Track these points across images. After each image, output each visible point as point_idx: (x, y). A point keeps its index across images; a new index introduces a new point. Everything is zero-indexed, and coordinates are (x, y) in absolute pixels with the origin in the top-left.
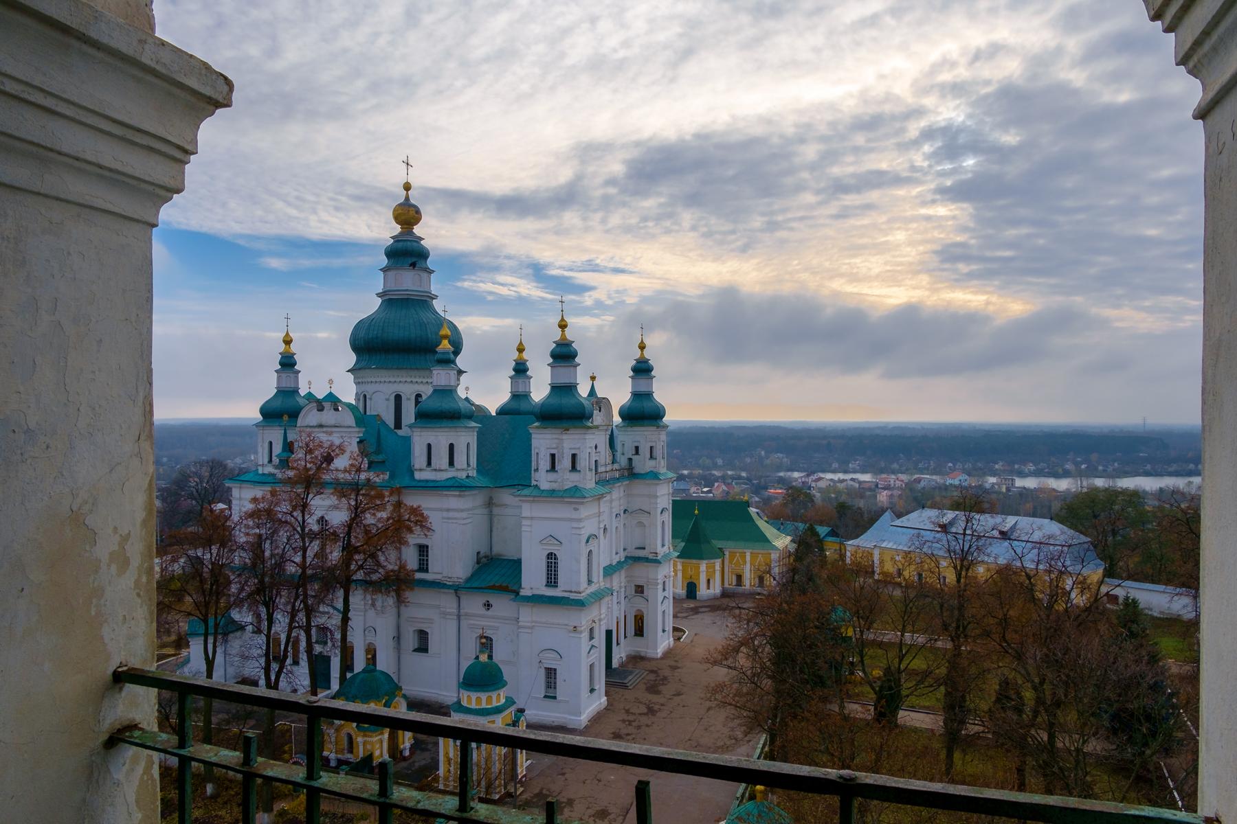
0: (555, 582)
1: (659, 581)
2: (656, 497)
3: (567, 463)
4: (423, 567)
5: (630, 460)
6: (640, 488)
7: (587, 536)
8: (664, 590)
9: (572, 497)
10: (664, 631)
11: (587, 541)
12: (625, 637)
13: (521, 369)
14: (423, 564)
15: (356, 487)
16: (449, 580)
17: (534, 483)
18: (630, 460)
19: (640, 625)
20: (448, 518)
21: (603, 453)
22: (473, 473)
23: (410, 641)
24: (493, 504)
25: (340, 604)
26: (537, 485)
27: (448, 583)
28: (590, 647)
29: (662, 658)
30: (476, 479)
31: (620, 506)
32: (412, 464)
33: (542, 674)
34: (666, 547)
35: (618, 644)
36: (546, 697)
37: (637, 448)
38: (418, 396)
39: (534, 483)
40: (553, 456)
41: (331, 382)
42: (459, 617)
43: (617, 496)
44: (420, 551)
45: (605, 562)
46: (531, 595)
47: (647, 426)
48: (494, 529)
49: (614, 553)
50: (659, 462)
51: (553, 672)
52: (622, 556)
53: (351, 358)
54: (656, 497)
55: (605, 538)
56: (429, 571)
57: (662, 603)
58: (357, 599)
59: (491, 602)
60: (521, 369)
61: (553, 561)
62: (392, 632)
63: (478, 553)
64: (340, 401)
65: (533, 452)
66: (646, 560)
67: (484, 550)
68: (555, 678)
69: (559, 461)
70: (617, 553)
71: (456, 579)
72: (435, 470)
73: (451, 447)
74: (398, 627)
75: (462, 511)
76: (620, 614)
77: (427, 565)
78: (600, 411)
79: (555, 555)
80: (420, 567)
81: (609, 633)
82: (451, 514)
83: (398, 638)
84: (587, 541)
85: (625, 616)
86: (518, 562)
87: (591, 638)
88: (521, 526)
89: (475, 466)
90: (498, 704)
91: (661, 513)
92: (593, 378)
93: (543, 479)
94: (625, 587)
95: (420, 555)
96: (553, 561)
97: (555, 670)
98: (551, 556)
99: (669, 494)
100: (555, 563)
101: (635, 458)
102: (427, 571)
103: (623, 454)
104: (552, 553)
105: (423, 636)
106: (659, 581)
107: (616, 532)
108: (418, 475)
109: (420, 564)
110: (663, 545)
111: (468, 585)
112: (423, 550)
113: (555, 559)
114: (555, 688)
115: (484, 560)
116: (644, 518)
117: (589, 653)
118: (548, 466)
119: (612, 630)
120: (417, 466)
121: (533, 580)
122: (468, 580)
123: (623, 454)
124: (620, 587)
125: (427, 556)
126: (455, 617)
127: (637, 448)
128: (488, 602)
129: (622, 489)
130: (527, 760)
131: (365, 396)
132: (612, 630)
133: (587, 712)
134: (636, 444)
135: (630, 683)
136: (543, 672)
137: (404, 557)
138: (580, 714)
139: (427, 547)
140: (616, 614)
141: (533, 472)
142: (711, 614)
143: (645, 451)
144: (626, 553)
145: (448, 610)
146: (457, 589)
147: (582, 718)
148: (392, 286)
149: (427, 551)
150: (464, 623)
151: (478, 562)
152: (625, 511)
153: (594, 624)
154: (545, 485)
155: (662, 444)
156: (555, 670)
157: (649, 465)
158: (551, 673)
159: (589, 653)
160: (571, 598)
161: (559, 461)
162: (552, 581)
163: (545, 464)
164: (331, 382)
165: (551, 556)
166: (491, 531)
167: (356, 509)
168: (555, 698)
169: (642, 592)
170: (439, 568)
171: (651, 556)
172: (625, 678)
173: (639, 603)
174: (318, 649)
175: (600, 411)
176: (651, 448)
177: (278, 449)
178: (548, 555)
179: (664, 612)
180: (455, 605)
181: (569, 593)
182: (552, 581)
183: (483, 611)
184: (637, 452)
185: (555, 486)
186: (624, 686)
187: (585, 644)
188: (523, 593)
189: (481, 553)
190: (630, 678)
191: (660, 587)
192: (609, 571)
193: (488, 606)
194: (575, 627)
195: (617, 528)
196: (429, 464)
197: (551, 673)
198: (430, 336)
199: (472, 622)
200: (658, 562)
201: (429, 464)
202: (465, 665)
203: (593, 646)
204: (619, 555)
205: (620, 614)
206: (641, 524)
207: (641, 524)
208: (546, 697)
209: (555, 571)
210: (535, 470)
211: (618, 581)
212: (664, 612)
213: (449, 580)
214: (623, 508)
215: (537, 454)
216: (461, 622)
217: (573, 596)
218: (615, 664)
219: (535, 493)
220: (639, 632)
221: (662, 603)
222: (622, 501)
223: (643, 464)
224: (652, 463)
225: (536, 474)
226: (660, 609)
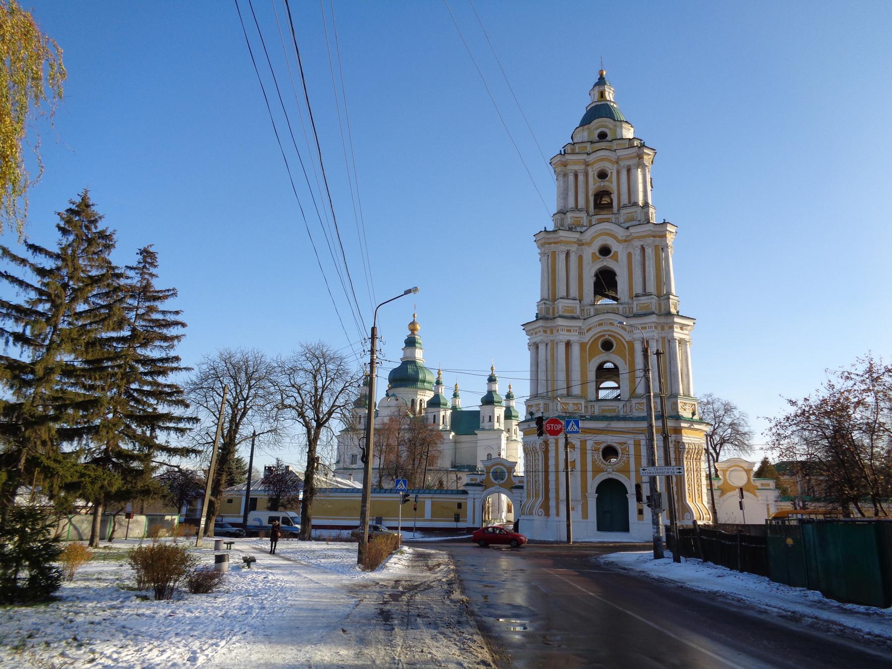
38: (421, 400)
40: (490, 417)
148: (408, 354)
163: (487, 419)
185: (491, 428)
196: (434, 422)
201: (434, 422)
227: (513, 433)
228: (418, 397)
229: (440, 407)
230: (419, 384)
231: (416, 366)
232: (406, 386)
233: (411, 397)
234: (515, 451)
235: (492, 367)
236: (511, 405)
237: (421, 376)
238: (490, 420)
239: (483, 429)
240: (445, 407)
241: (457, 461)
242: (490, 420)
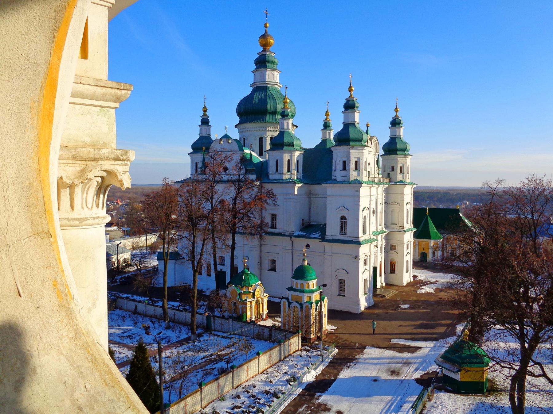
0: (345, 233)
3: (353, 166)
4: (274, 226)
8: (408, 248)
10: (407, 272)
11: (363, 210)
12: (385, 274)
13: (326, 126)
14: (274, 225)
15: (239, 181)
16: (287, 232)
17: (333, 178)
18: (389, 174)
19: (393, 267)
20: (287, 199)
23: (267, 265)
24: (311, 194)
25: (230, 243)
26: (335, 179)
27: (286, 234)
28: (364, 269)
29: (405, 286)
32: (268, 172)
35: (380, 275)
39: (333, 178)
40: (344, 162)
41: (226, 128)
42: (292, 253)
44: (272, 218)
45: (373, 229)
46: (331, 239)
48: (312, 208)
49: (379, 224)
50: (406, 176)
53: (237, 120)
55: (374, 216)
56: (277, 227)
57: (406, 255)
58: (238, 238)
60: (326, 126)
61: (344, 220)
62: (257, 260)
63: (303, 220)
64: (230, 138)
65: (333, 161)
67: (306, 218)
68: (344, 285)
69: (348, 164)
71: (291, 232)
72: (280, 174)
73: (289, 162)
74: (261, 258)
76: (381, 259)
77: (276, 225)
78: (372, 144)
79: (345, 217)
80: (272, 227)
81: (375, 269)
83: (260, 264)
84: (363, 210)
85: (385, 262)
89: (302, 173)
90: (313, 288)
91: (407, 204)
92: (367, 125)
93: (338, 174)
95: (272, 220)
96: (344, 220)
98: (343, 218)
100: (345, 221)
101: (392, 173)
102: (276, 228)
104: (343, 216)
105: (273, 262)
108: (271, 177)
109: (272, 225)
112: (274, 217)
113: (345, 220)
114: (344, 291)
115: (306, 224)
117: (364, 272)
118: (341, 167)
120: (270, 172)
121: (333, 230)
123: (385, 171)
125: (276, 220)
128: (308, 244)
131: (244, 139)
137: (263, 216)
139: (276, 215)
140: (379, 260)
141: (333, 172)
149: (276, 218)
151: (303, 224)
153: (366, 257)
154: (339, 179)
157: (400, 177)
158: (342, 283)
159: (364, 272)
160: (354, 240)
161: (348, 164)
162: (343, 231)
163: (340, 166)
164: (226, 128)
165: (343, 218)
166: (310, 209)
167: (239, 189)
168: (344, 296)
170: (281, 226)
173: (393, 255)
174: (219, 268)
175: (372, 144)
176: (401, 167)
177: (200, 165)
178: (341, 217)
179: (407, 261)
180: (290, 245)
181: (352, 238)
182: (343, 231)
184: (393, 169)
185: (345, 178)
188: (327, 238)
189: (305, 220)
191: (405, 246)
193: (308, 246)
194: (356, 257)
196: (277, 170)
198: (278, 106)
201: (277, 170)
202: (295, 267)
204: (381, 226)
205: (381, 259)
208: (339, 295)
209: (345, 226)
210: (334, 171)
212: (407, 261)
213: (287, 232)
215: (336, 161)
217: (354, 239)
218: (379, 286)
220: (393, 271)
221: (406, 255)
225: (335, 172)
227: (399, 171)
228: (268, 133)
229: (282, 149)
230: (269, 117)
231: (265, 95)
232: (251, 121)
233: (258, 134)
234: (400, 196)
235: (350, 87)
236: (397, 134)
237: (269, 107)
238: (344, 169)
239: (335, 181)
240: (291, 148)
241: (311, 218)
242: (344, 169)
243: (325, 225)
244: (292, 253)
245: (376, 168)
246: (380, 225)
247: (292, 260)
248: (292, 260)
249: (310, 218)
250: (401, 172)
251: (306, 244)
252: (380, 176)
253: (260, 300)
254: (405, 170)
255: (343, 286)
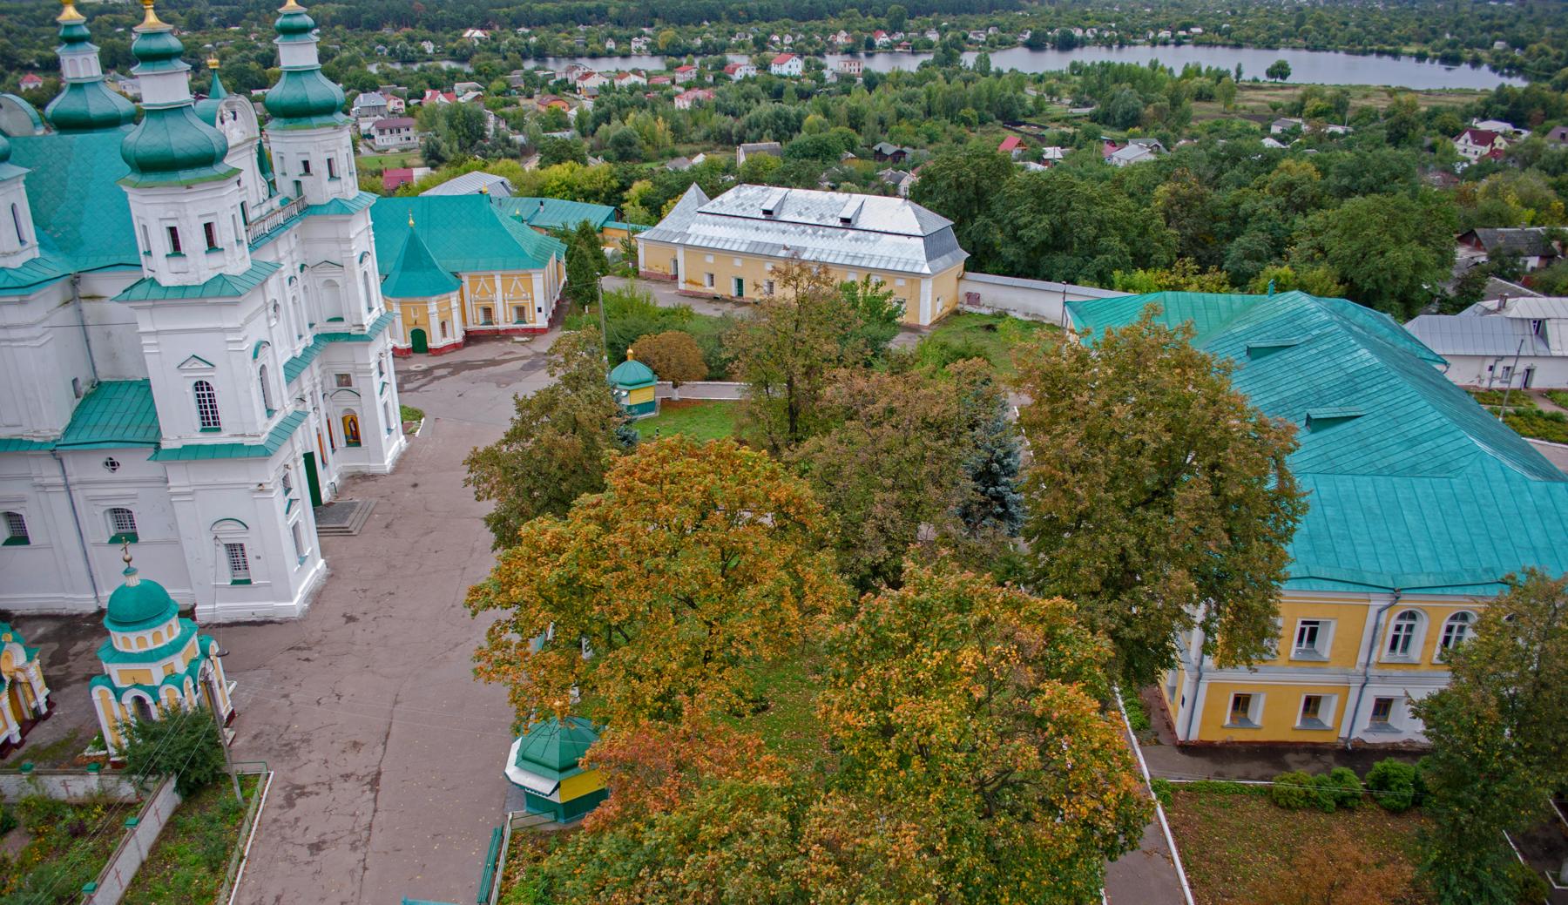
1: (372, 366)
2: (349, 241)
5: (298, 183)
6: (319, 229)
7: (254, 345)
9: (218, 296)
18: (298, 183)
21: (252, 187)
22: (37, 253)
27: (35, 440)
30: (41, 262)
31: (293, 263)
33: (223, 553)
34: (376, 309)
36: (235, 582)
37: (306, 164)
42: (67, 487)
43: (286, 252)
47: (321, 126)
49: (296, 337)
50: (346, 184)
51: (239, 552)
52: (309, 339)
54: (349, 241)
59: (115, 460)
63: (75, 381)
66: (348, 336)
67: (84, 377)
70: (300, 337)
75: (32, 325)
82: (14, 334)
86: (145, 386)
87: (288, 490)
88: (141, 347)
91: (361, 262)
94: (322, 383)
97: (241, 545)
99: (368, 228)
101: (305, 180)
103: (284, 174)
106: (372, 366)
107: (294, 303)
110: (370, 309)
111: (71, 439)
116: (333, 274)
117: (288, 512)
119: (312, 454)
122: (70, 428)
123: (284, 174)
124: (315, 386)
126: (62, 489)
127: (306, 164)
129: (292, 236)
130: (228, 685)
132: (312, 454)
133: (300, 590)
134: (305, 158)
135: (354, 525)
136: (223, 551)
138: (291, 600)
142: (451, 379)
143: (320, 167)
144: (315, 331)
145: (47, 481)
146: (55, 451)
147: (294, 603)
150: (78, 495)
151: (77, 397)
152: (302, 267)
155: (347, 151)
156: (241, 545)
159: (288, 512)
166: (87, 341)
168: (248, 582)
169: (349, 383)
171: (354, 331)
172: (345, 518)
173: (346, 401)
176: (329, 161)
179: (386, 406)
180: (57, 471)
183: (106, 474)
186: (346, 532)
187: (278, 499)
190: (352, 516)
192: (293, 369)
193: (112, 465)
195: (294, 298)
197: (236, 551)
199: (90, 492)
200: (364, 339)
203: (291, 501)
206: (331, 284)
207: (331, 284)
208: (235, 582)
211: (311, 378)
214: (298, 266)
216: (73, 494)
219: (154, 292)
222: (295, 254)
223: (320, 190)
224: (335, 186)
226: (379, 402)
243: (148, 380)
244: (67, 487)
245: (259, 182)
246: (300, 337)
247: (74, 508)
248: (74, 508)
249: (94, 368)
250: (332, 176)
251: (105, 459)
252: (276, 203)
253: (21, 677)
254: (341, 166)
255: (240, 558)
